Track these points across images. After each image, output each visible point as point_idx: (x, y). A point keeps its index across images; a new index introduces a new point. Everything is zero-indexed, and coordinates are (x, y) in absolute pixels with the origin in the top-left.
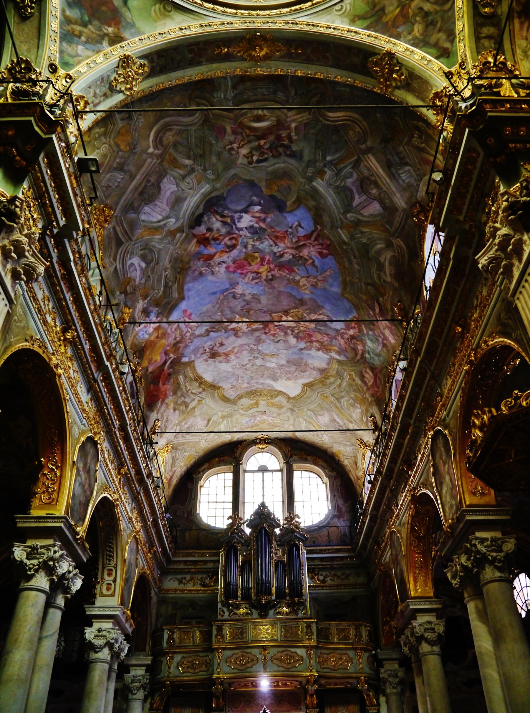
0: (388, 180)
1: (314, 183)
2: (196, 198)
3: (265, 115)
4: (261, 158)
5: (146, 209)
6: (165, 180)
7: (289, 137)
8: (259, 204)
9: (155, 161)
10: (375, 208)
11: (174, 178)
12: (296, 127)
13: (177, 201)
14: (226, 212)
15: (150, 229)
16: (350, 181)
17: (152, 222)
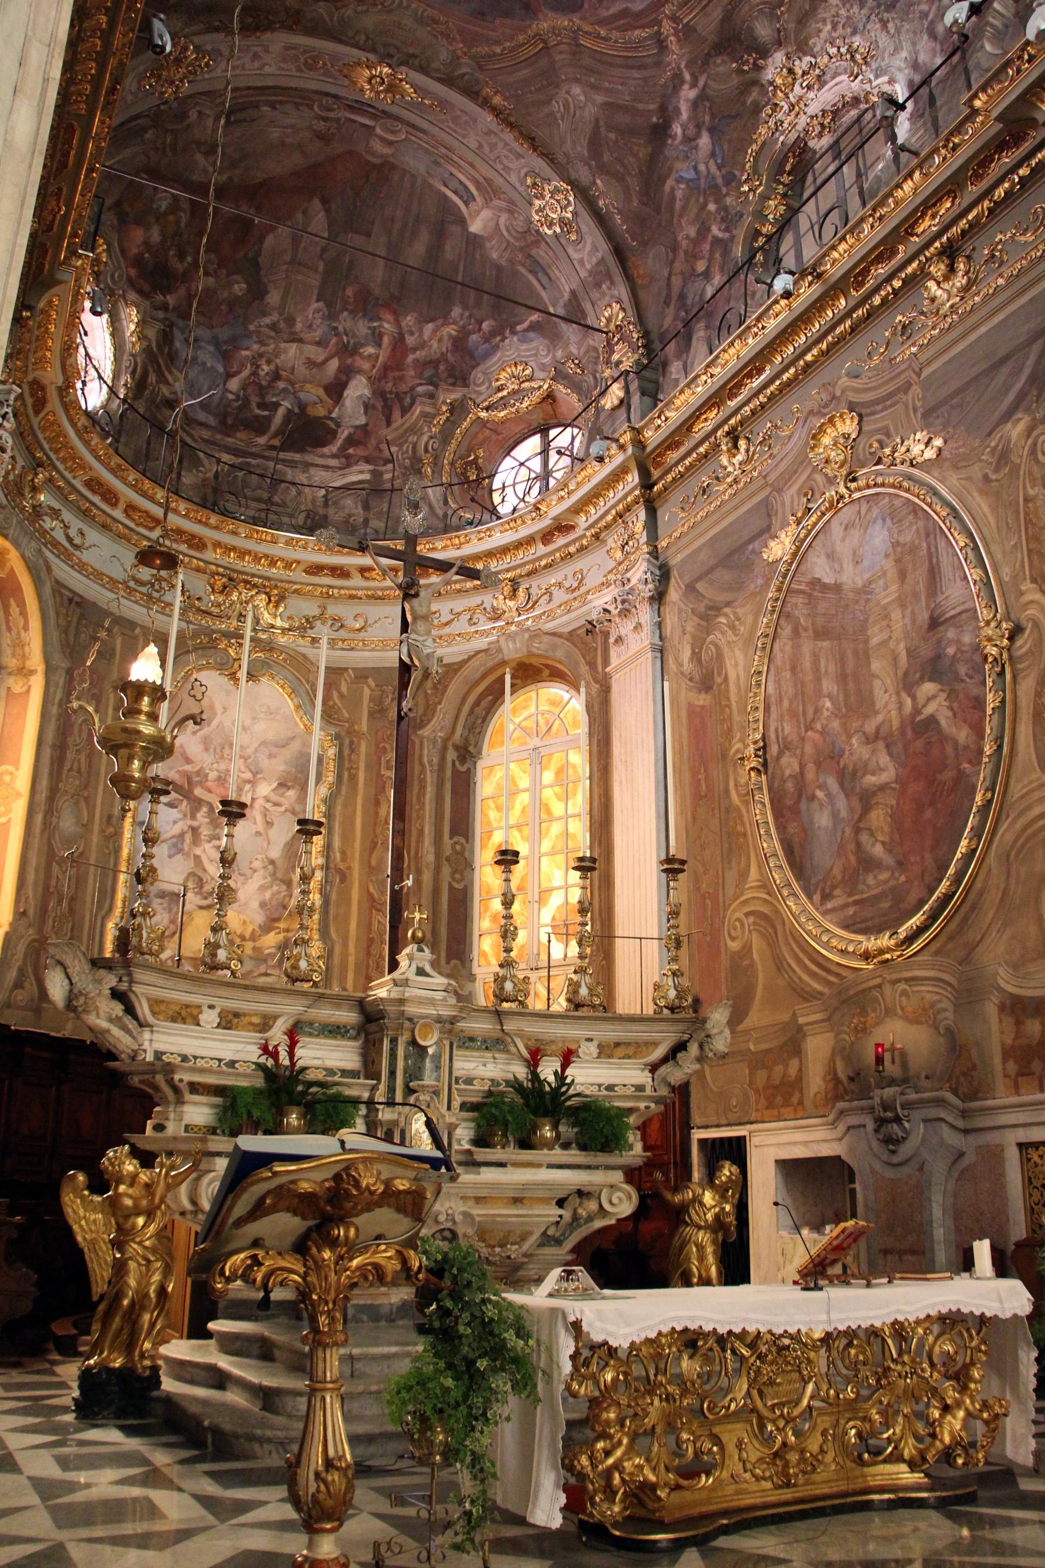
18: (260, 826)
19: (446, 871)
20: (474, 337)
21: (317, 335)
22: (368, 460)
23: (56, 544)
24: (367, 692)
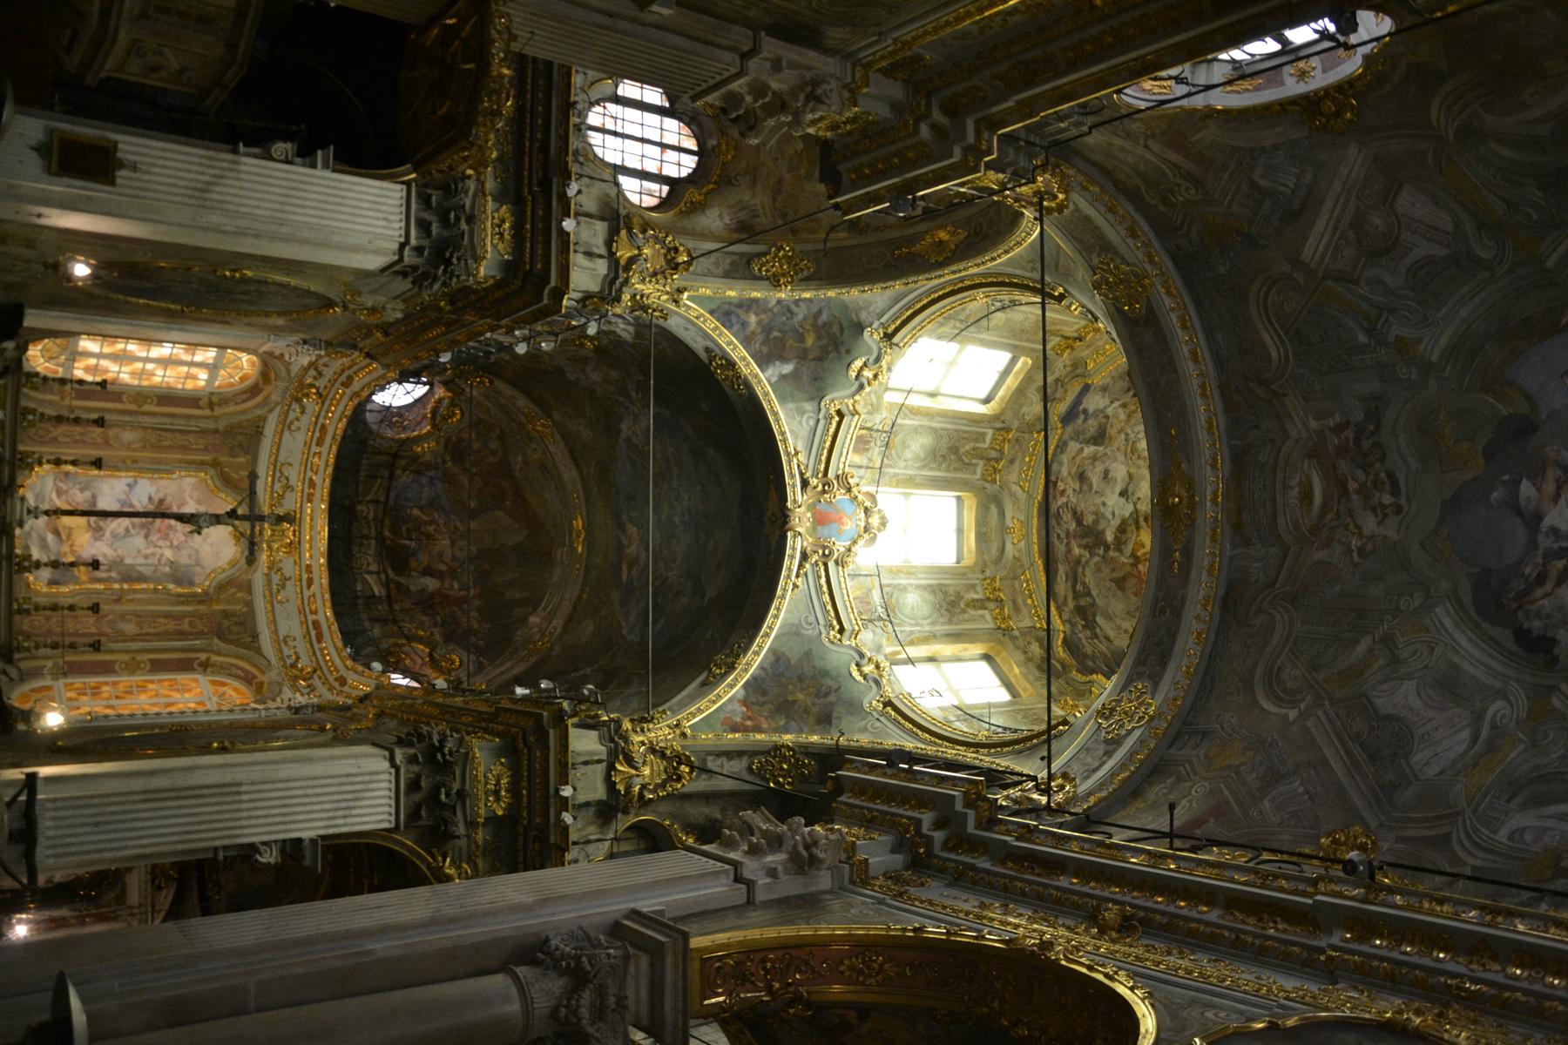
0: (1329, 205)
1: (1434, 358)
2: (1464, 642)
3: (1301, 481)
4: (1388, 486)
5: (1417, 759)
6: (1378, 702)
7: (1339, 429)
8: (1515, 484)
9: (1320, 713)
10: (1410, 203)
11: (1383, 682)
12: (1317, 419)
13: (1450, 686)
14: (1527, 571)
15: (1475, 765)
16: (1388, 280)
17: (1465, 753)
18: (144, 552)
19: (125, 657)
20: (473, 639)
21: (458, 554)
22: (389, 596)
23: (286, 414)
24: (238, 607)
